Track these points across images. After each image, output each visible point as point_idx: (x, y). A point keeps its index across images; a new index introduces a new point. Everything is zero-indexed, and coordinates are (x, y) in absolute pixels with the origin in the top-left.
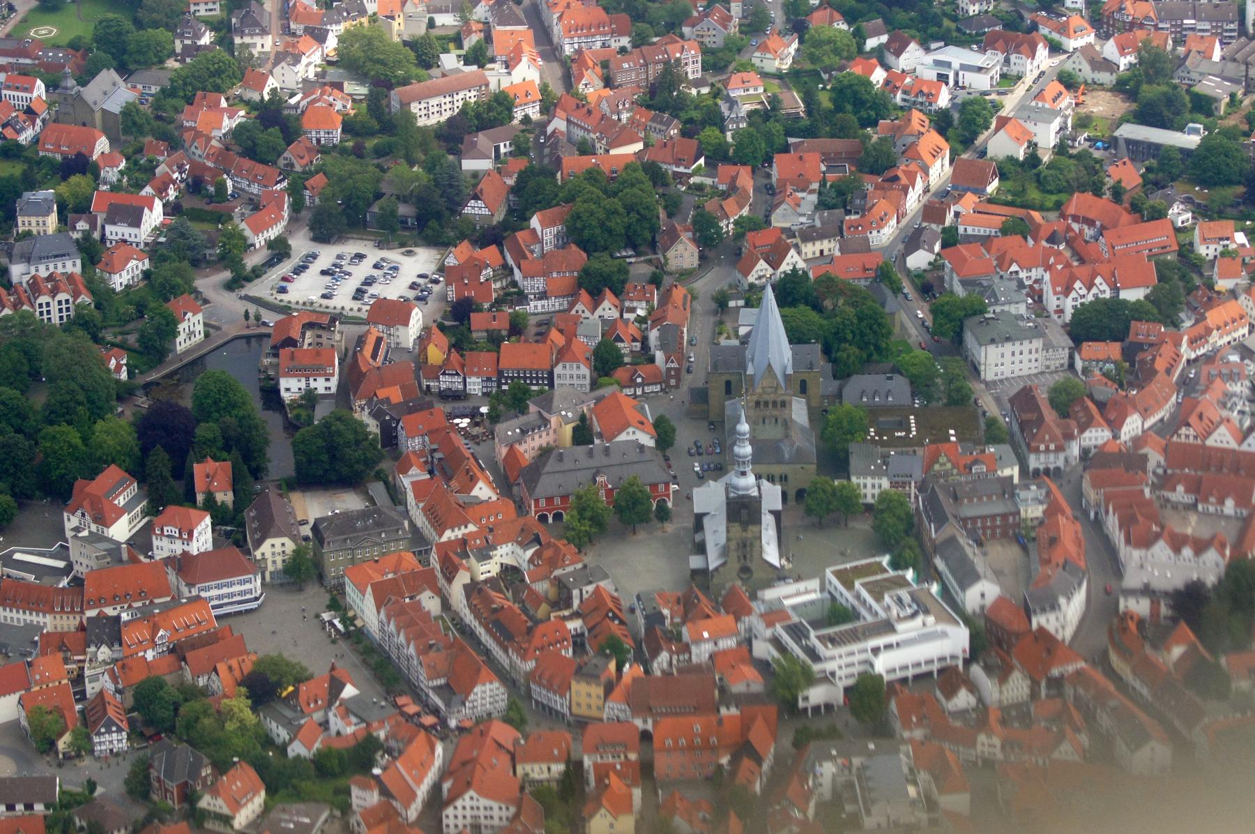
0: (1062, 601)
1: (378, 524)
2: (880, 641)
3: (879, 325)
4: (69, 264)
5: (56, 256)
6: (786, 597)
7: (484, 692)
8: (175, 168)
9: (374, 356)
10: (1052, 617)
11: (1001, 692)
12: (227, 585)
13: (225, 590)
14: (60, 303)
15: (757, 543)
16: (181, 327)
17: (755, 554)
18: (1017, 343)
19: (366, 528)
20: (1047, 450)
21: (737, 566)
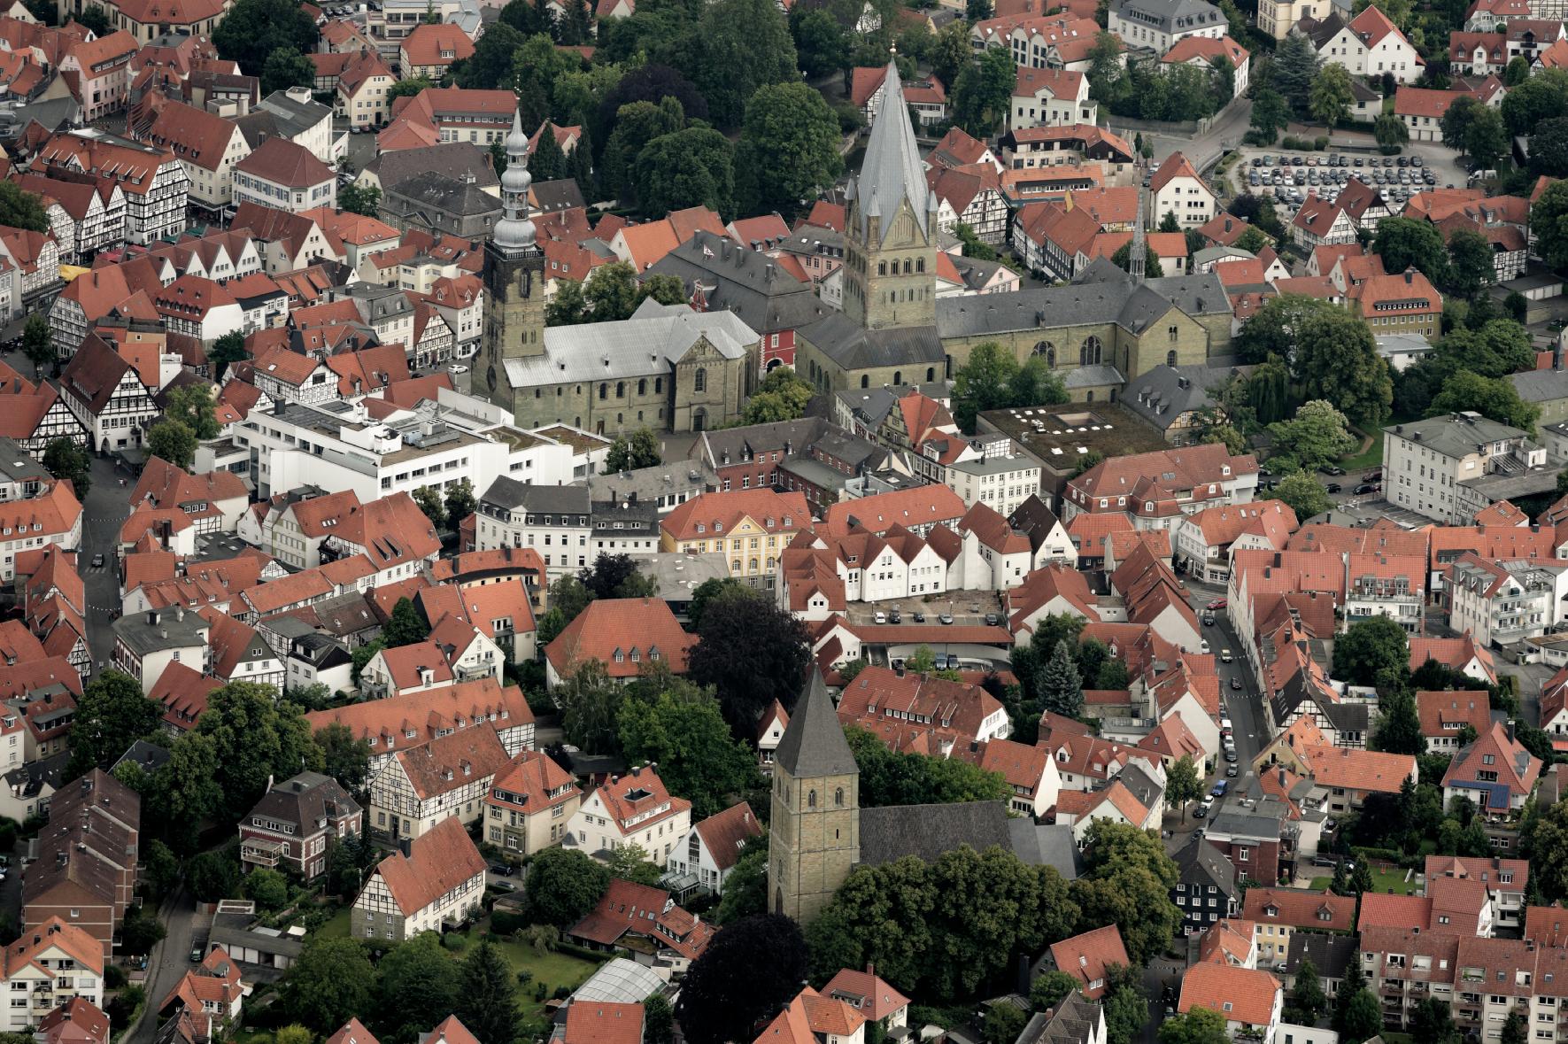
0: (519, 512)
1: (442, 203)
2: (315, 438)
3: (1333, 353)
4: (1158, 35)
5: (1147, 18)
6: (456, 412)
7: (69, 313)
8: (1520, 35)
9: (1020, 185)
10: (500, 526)
11: (274, 537)
12: (267, 190)
13: (262, 196)
14: (1036, 49)
15: (500, 332)
16: (1017, 102)
17: (499, 352)
18: (1429, 452)
19: (429, 200)
20: (1077, 502)
21: (487, 364)
